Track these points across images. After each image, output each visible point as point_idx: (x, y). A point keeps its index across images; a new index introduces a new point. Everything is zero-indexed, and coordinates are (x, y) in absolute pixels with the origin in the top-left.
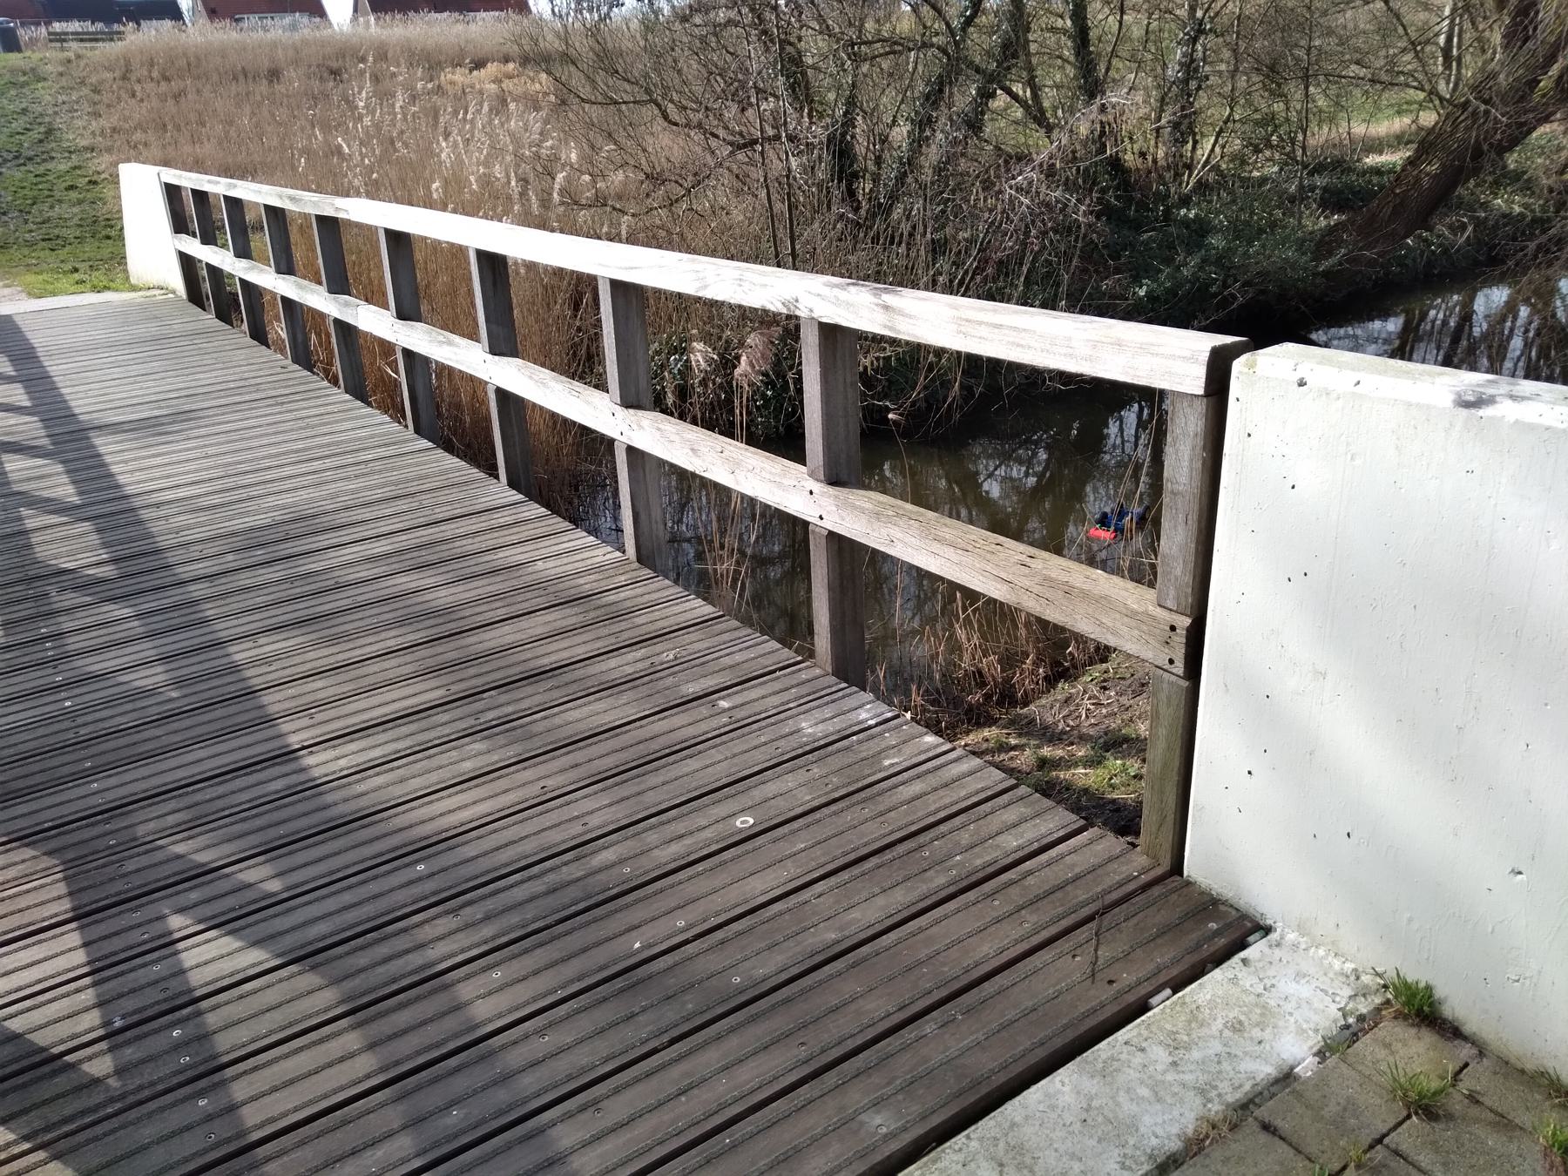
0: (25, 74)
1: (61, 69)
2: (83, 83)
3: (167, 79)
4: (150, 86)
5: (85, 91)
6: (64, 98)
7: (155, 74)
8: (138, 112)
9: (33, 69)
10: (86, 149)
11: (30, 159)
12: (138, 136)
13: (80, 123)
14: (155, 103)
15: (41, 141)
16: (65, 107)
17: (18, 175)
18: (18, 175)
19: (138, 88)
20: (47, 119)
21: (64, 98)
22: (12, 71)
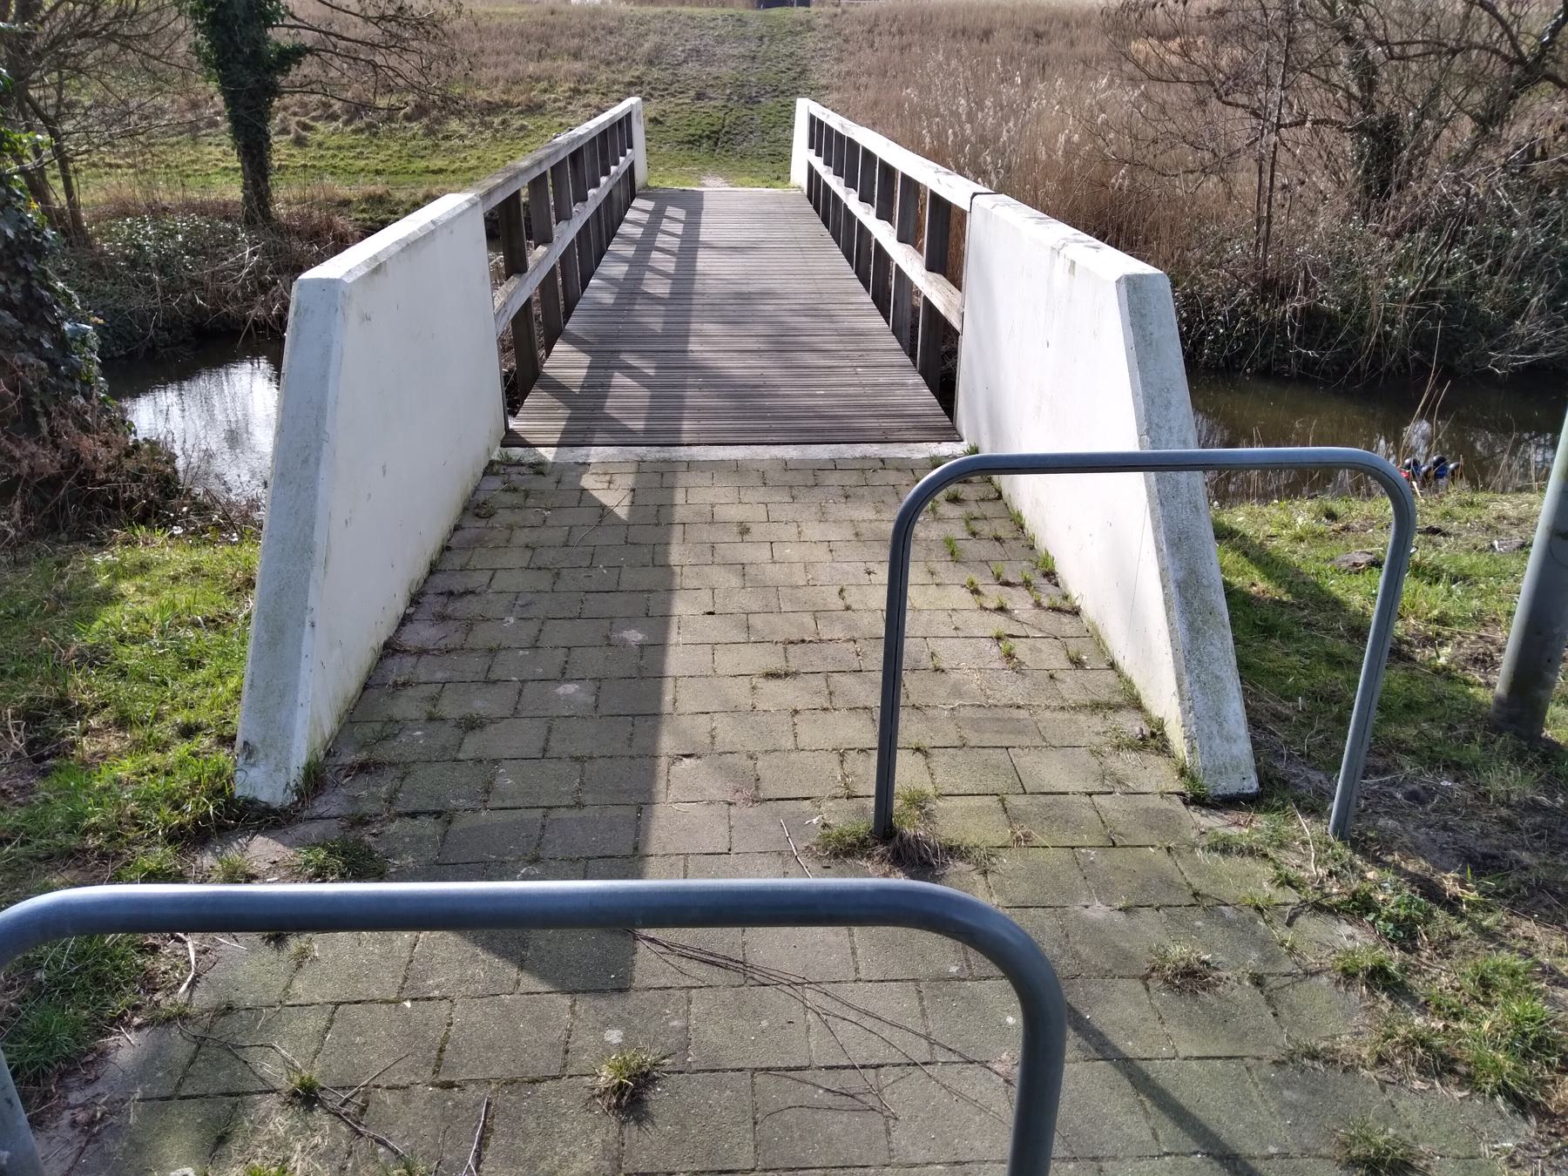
0: (802, 24)
1: (827, 22)
2: (839, 34)
3: (901, 33)
4: (886, 38)
5: (839, 40)
6: (822, 45)
7: (894, 29)
8: (868, 58)
9: (808, 21)
10: (823, 87)
11: (783, 92)
12: (864, 80)
13: (826, 66)
14: (886, 53)
15: (795, 79)
16: (821, 53)
17: (771, 104)
18: (771, 104)
19: (877, 40)
20: (805, 62)
21: (822, 45)
22: (794, 22)
